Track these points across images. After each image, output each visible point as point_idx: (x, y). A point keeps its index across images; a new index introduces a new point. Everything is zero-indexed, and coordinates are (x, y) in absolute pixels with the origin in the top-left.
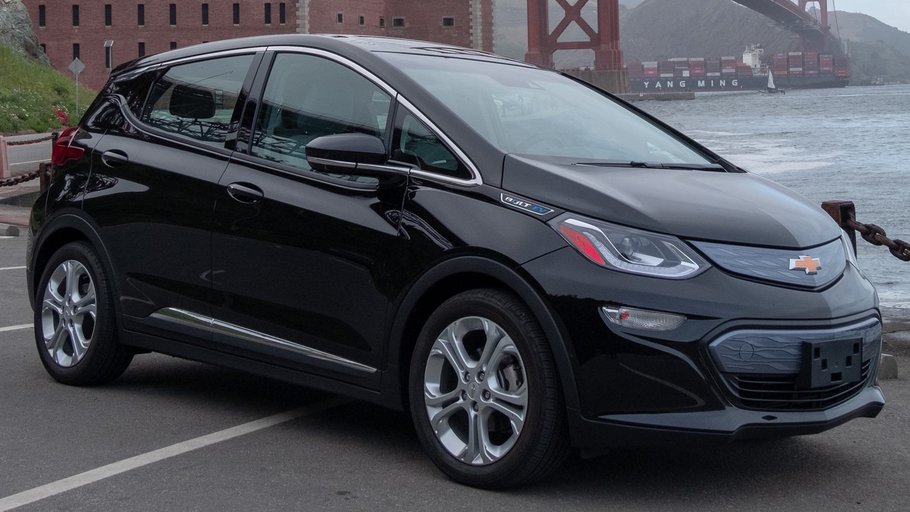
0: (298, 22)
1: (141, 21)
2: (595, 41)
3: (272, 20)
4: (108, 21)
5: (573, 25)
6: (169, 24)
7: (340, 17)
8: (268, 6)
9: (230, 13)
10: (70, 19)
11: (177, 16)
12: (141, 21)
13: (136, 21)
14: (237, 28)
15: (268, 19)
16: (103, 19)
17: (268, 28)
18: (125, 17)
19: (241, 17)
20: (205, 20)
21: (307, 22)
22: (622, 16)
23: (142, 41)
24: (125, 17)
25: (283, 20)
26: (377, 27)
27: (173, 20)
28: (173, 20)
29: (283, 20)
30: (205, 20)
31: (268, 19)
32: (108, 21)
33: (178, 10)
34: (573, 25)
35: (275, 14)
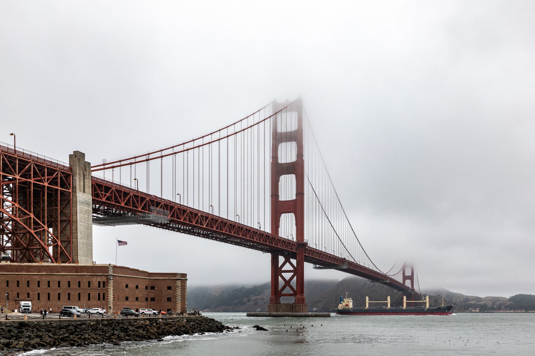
0: (109, 287)
1: (59, 286)
2: (295, 294)
3: (101, 287)
4: (49, 286)
5: (288, 288)
6: (68, 287)
7: (127, 286)
8: (99, 282)
9: (87, 284)
10: (37, 285)
11: (71, 285)
12: (59, 286)
13: (57, 286)
14: (89, 289)
15: (99, 286)
16: (47, 285)
17: (99, 289)
18: (54, 285)
19: (91, 285)
20: (79, 286)
21: (112, 287)
22: (305, 286)
23: (59, 292)
24: (54, 285)
25: (104, 287)
26: (144, 289)
27: (69, 286)
28: (69, 286)
29: (104, 287)
30: (79, 286)
31: (99, 286)
32: (49, 286)
33: (71, 283)
34: (288, 288)
35: (102, 285)
